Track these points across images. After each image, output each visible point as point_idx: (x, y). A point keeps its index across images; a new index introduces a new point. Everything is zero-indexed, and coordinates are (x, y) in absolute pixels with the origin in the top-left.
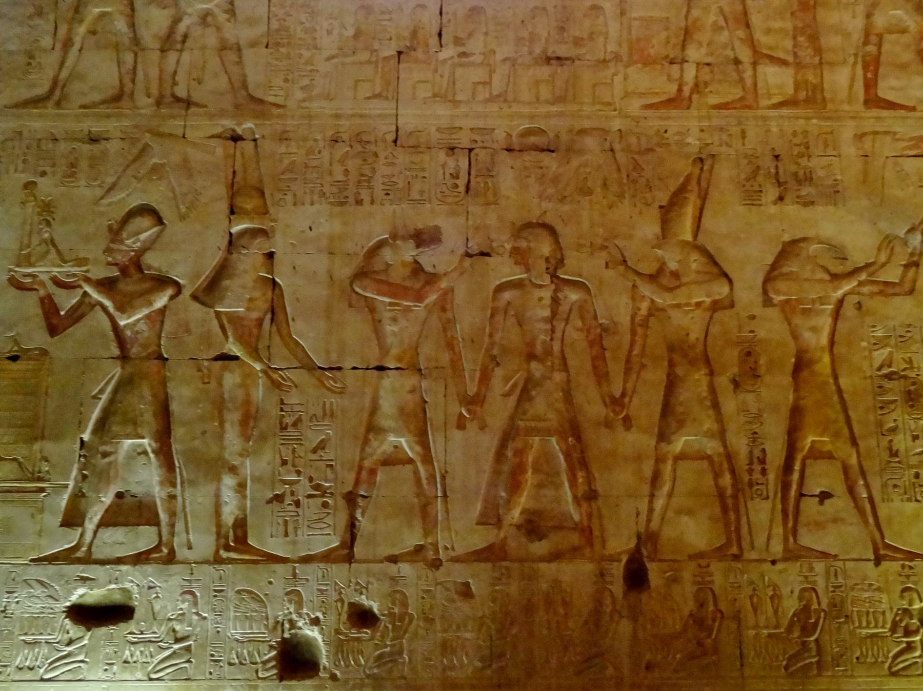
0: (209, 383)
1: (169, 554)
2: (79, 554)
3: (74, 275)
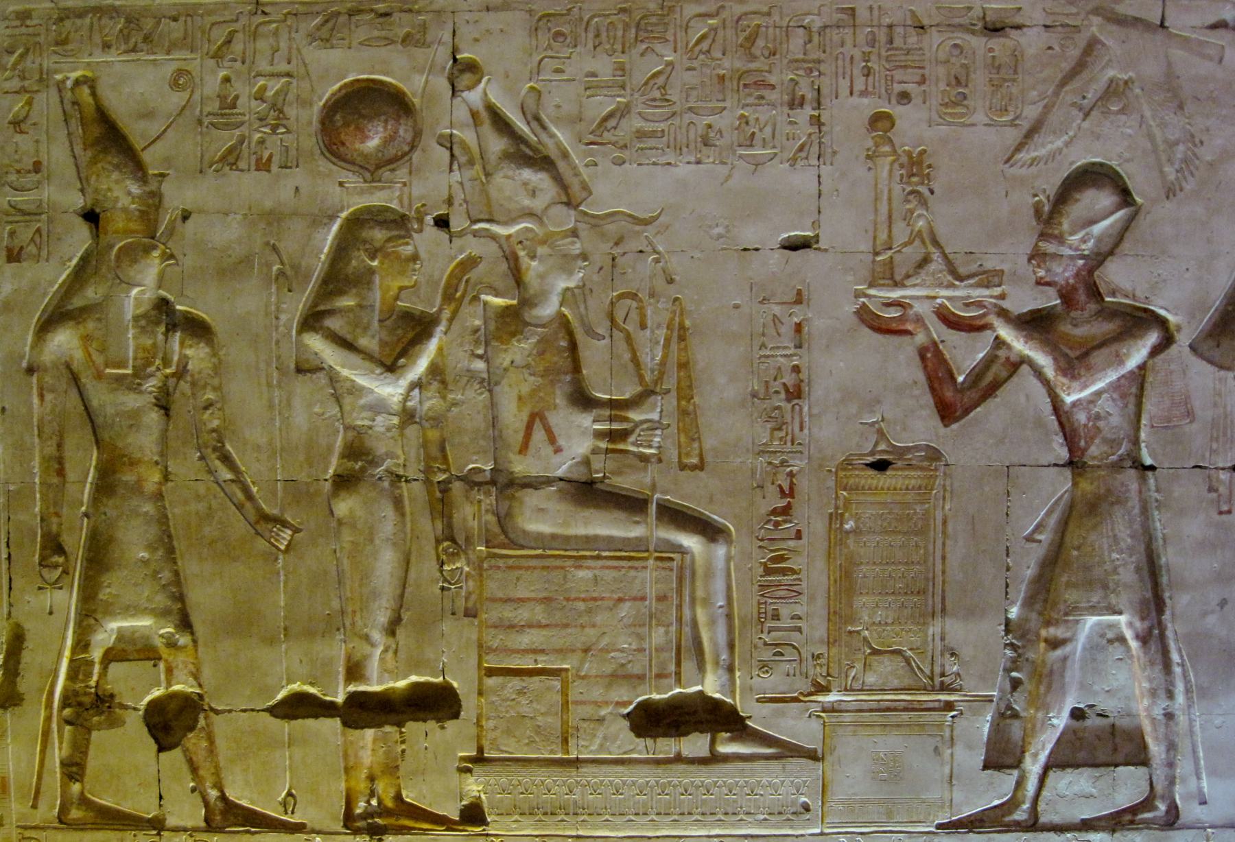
2: (1020, 815)
3: (980, 304)
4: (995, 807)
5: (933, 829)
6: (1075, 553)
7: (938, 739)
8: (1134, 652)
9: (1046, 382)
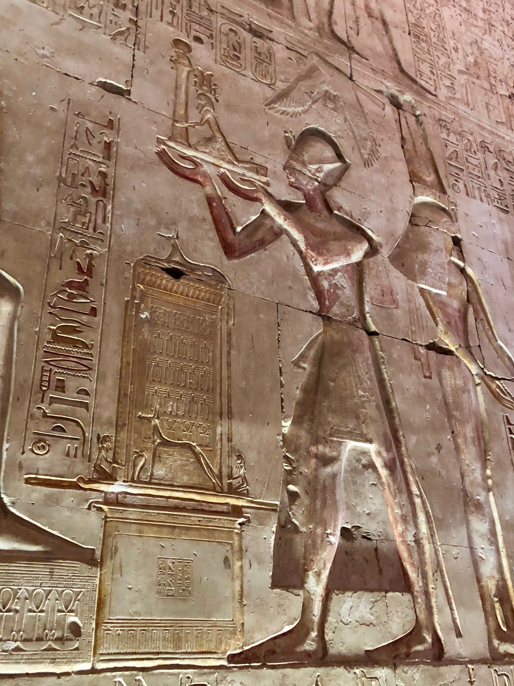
0: (430, 377)
1: (433, 643)
2: (310, 645)
3: (251, 183)
4: (284, 634)
5: (224, 663)
6: (332, 384)
7: (228, 548)
8: (384, 480)
9: (300, 252)
